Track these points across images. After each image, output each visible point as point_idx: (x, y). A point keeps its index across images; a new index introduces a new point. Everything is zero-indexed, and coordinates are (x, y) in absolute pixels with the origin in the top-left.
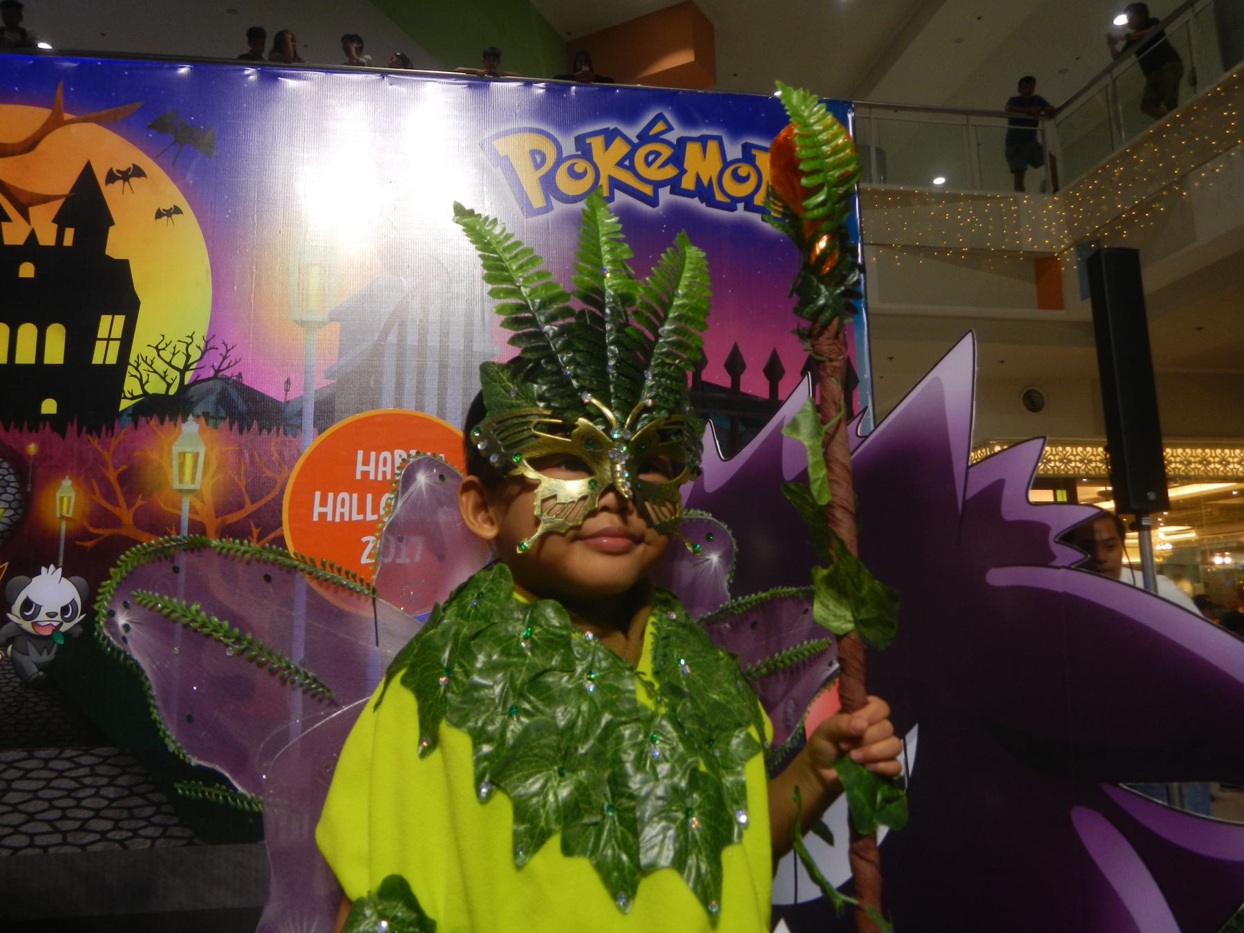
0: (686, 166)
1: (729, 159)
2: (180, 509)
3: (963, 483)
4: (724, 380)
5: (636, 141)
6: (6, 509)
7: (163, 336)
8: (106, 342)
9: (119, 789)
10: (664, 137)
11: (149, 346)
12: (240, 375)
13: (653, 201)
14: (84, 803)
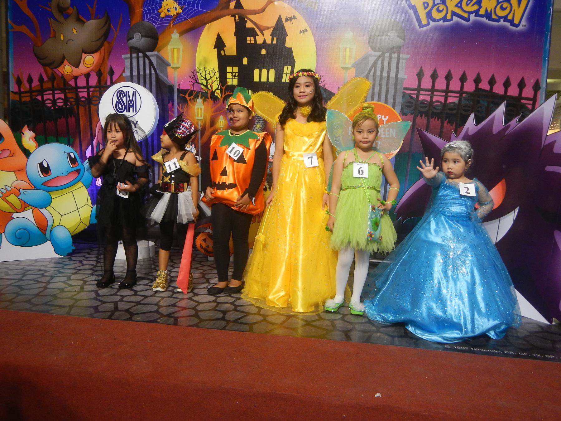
0: (482, 5)
3: (544, 140)
4: (487, 87)
12: (324, 86)
13: (467, 20)
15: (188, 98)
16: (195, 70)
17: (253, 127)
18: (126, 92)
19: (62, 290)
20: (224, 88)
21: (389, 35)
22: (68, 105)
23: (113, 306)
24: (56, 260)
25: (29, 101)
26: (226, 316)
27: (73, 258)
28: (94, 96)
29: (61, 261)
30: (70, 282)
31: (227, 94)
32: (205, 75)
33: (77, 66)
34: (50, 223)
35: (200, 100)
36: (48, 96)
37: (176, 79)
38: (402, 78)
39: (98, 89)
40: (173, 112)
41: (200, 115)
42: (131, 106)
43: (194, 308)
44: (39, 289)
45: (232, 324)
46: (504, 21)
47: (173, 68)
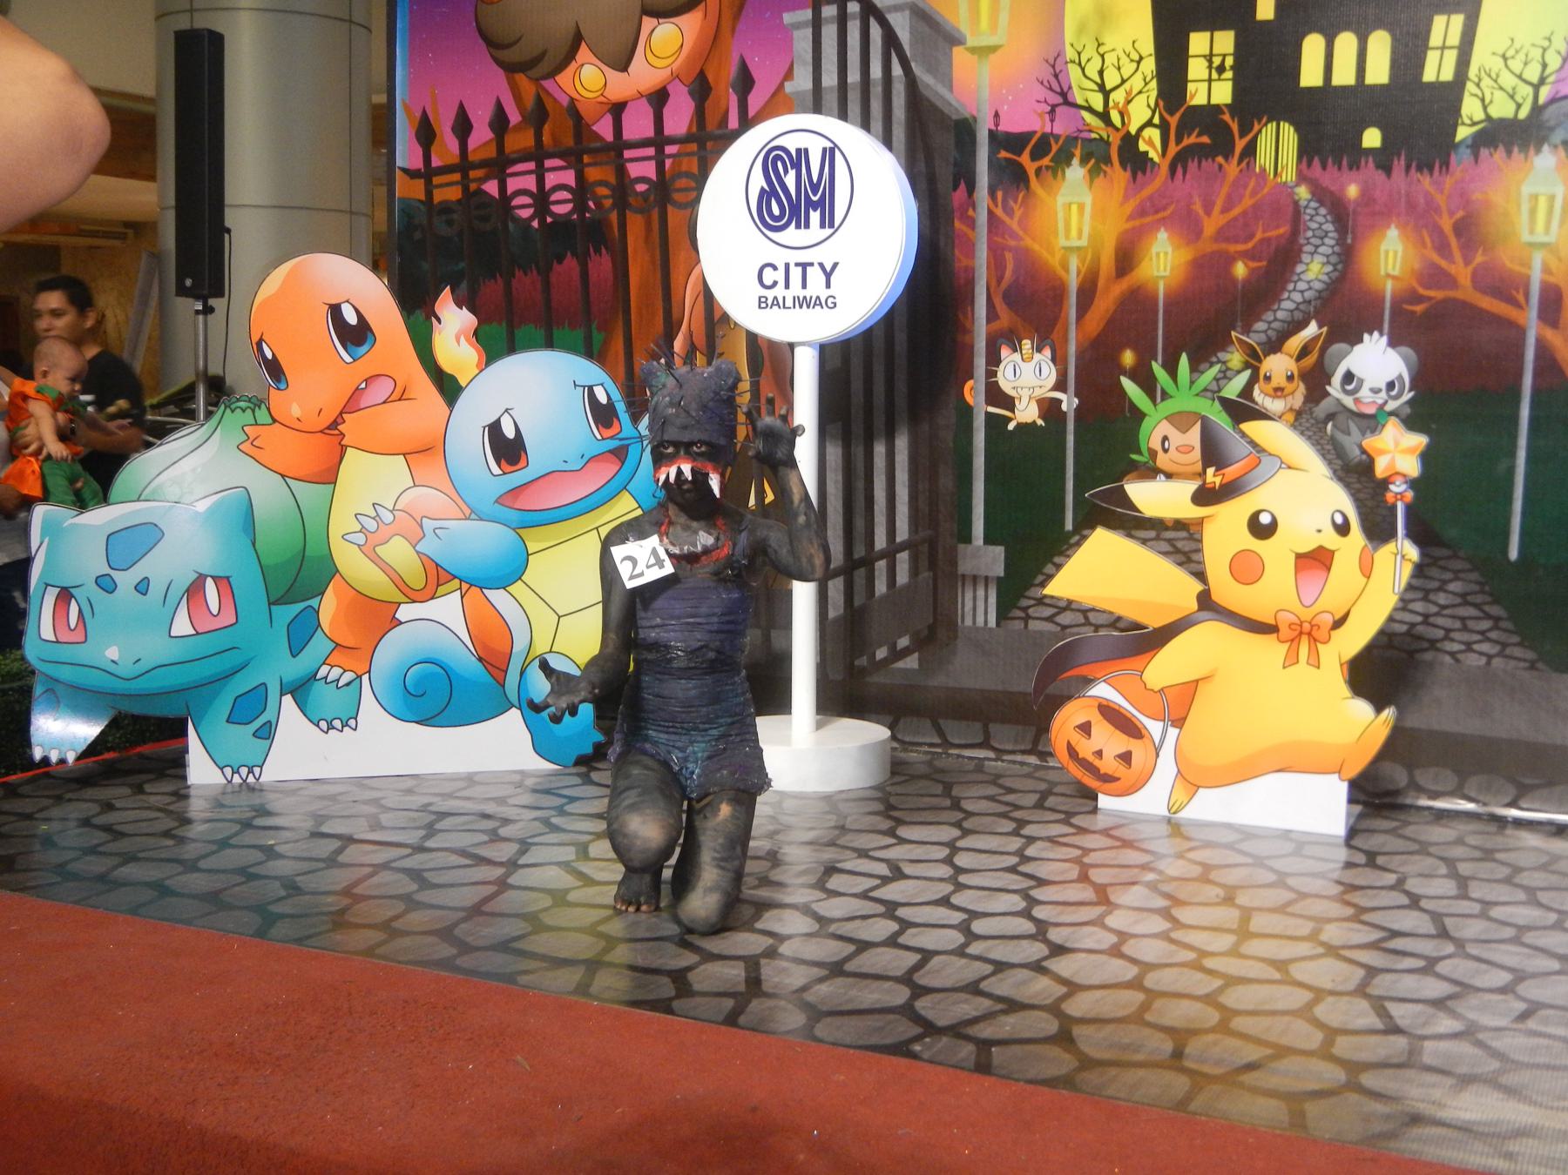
2: (1530, 268)
6: (1324, 264)
7: (1512, 40)
8: (1439, 52)
9: (1450, 596)
11: (1494, 54)
14: (1412, 606)
15: (1030, 167)
16: (1060, 54)
17: (1293, 272)
18: (799, 151)
19: (559, 898)
20: (1174, 121)
22: (588, 209)
23: (743, 974)
24: (538, 780)
25: (459, 201)
26: (1187, 1050)
27: (595, 776)
28: (680, 175)
29: (553, 786)
30: (586, 868)
31: (1187, 141)
32: (1101, 73)
33: (622, 63)
34: (520, 645)
35: (1076, 172)
36: (522, 181)
37: (985, 94)
39: (694, 147)
40: (972, 224)
41: (1074, 233)
42: (815, 206)
43: (1055, 1009)
44: (480, 887)
45: (1216, 1088)
47: (973, 50)
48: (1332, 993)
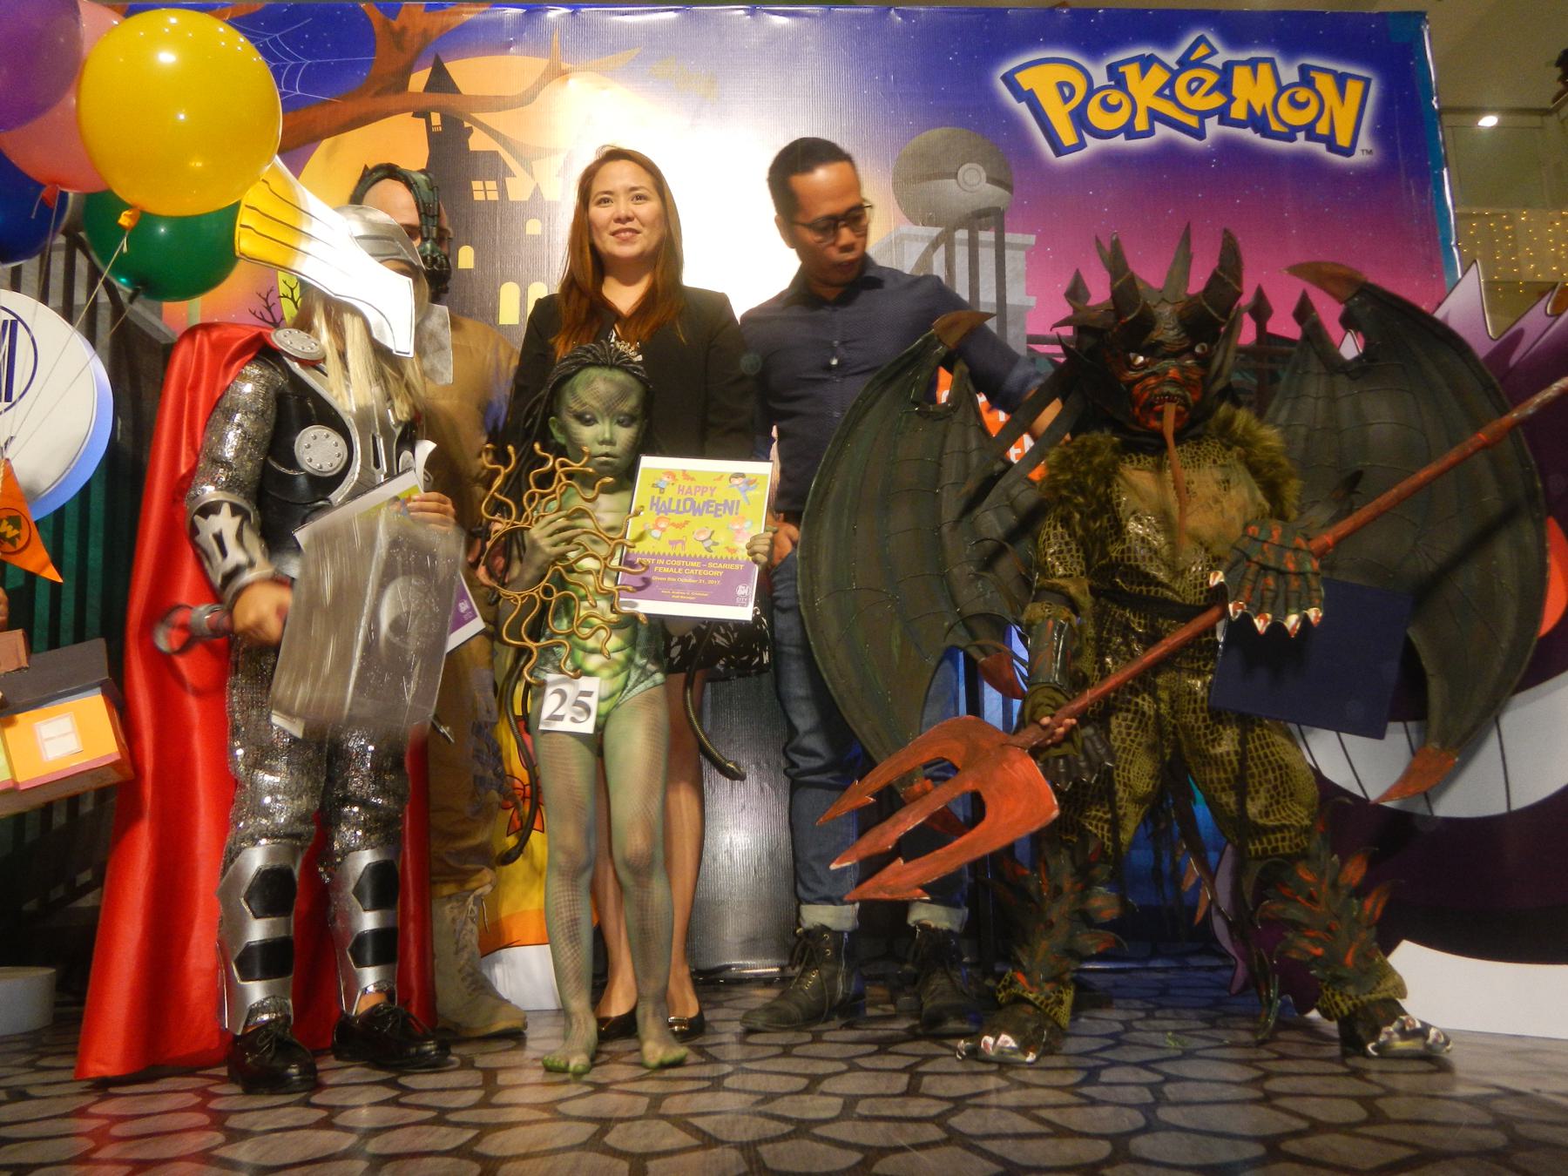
0: (1235, 93)
1: (1284, 82)
4: (1293, 331)
5: (1176, 67)
10: (1208, 61)
13: (1199, 133)
16: (273, 290)
21: (960, 172)
38: (1021, 307)
46: (1308, 138)
48: (622, 1120)
